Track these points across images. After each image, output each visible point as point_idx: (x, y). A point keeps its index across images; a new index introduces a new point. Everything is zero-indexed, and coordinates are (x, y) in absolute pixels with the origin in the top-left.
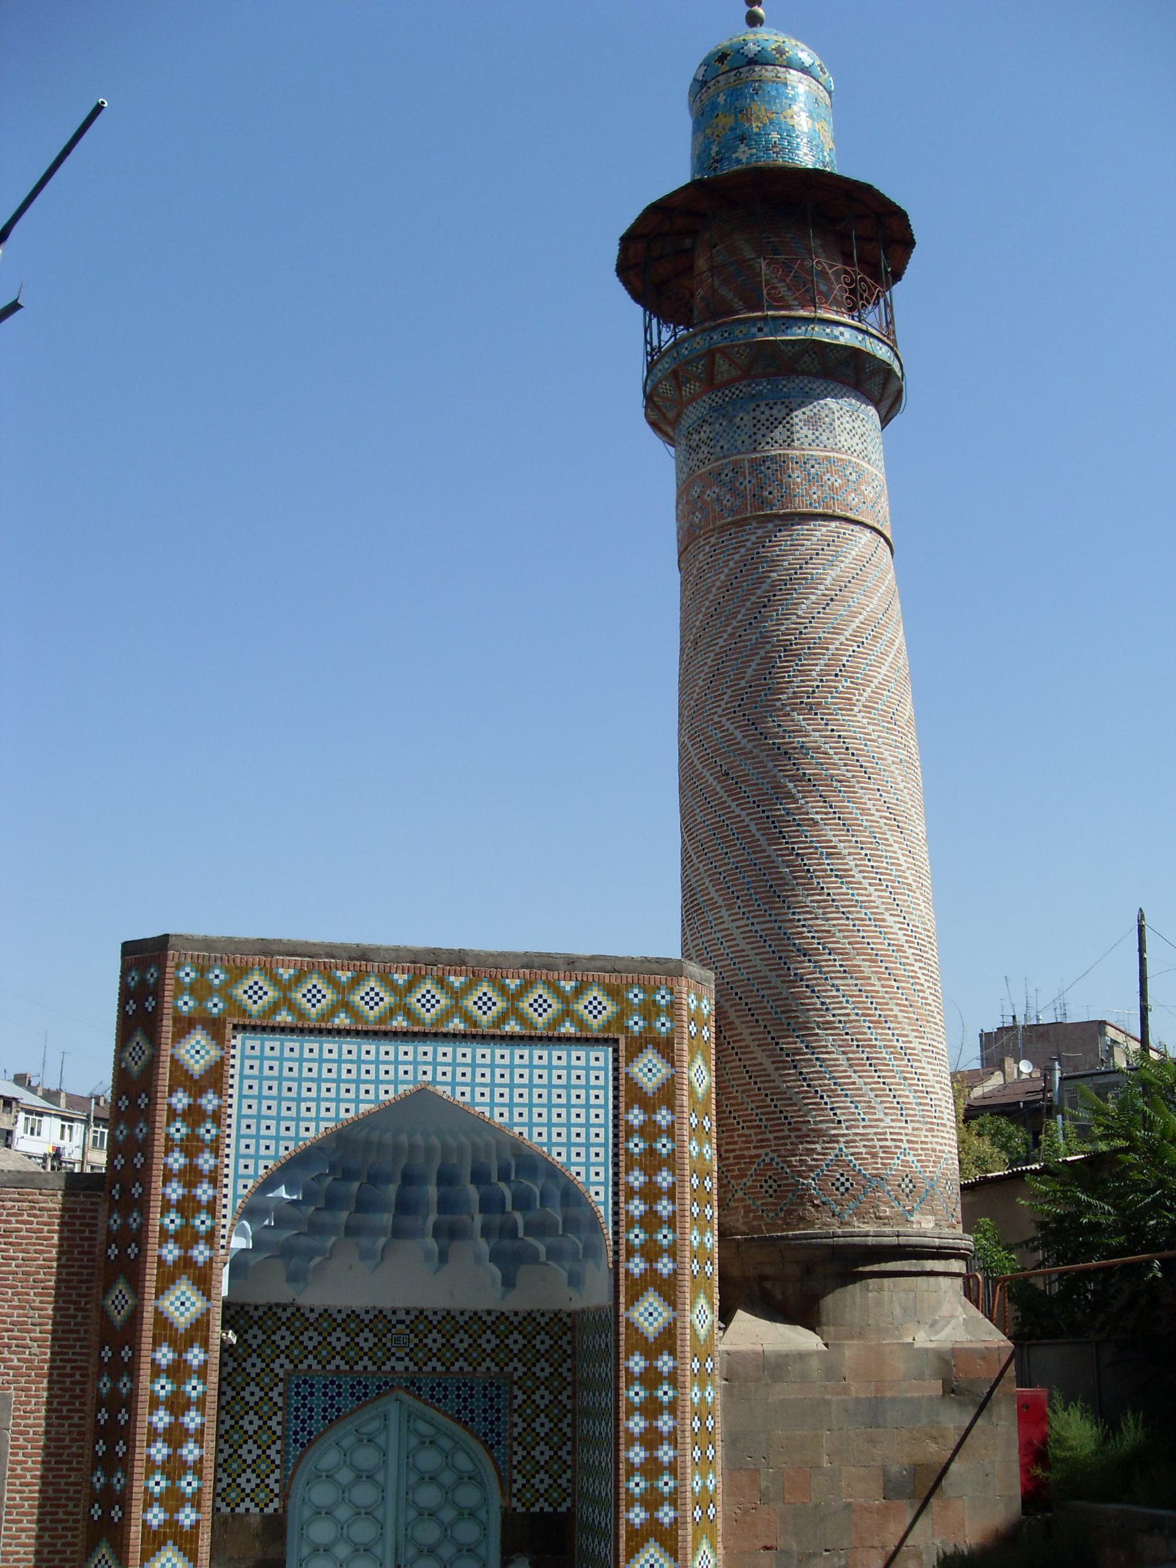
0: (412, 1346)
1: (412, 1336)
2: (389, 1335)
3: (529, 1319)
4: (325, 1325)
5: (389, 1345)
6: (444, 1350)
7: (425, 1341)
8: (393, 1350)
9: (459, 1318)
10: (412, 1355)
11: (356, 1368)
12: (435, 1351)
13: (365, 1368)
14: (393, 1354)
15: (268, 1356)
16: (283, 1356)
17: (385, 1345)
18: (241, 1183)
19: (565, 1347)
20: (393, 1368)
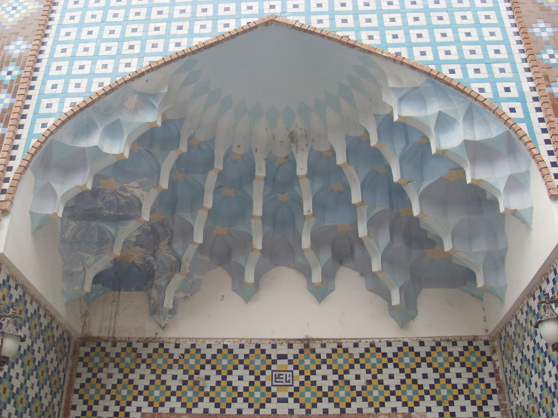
0: (296, 384)
1: (296, 372)
2: (268, 373)
3: (439, 349)
4: (192, 362)
5: (268, 384)
6: (336, 388)
7: (313, 378)
8: (274, 389)
9: (352, 350)
10: (296, 395)
11: (228, 411)
12: (325, 389)
13: (240, 411)
14: (274, 395)
15: (124, 397)
16: (141, 398)
17: (263, 384)
18: (40, 121)
19: (488, 380)
20: (274, 411)
